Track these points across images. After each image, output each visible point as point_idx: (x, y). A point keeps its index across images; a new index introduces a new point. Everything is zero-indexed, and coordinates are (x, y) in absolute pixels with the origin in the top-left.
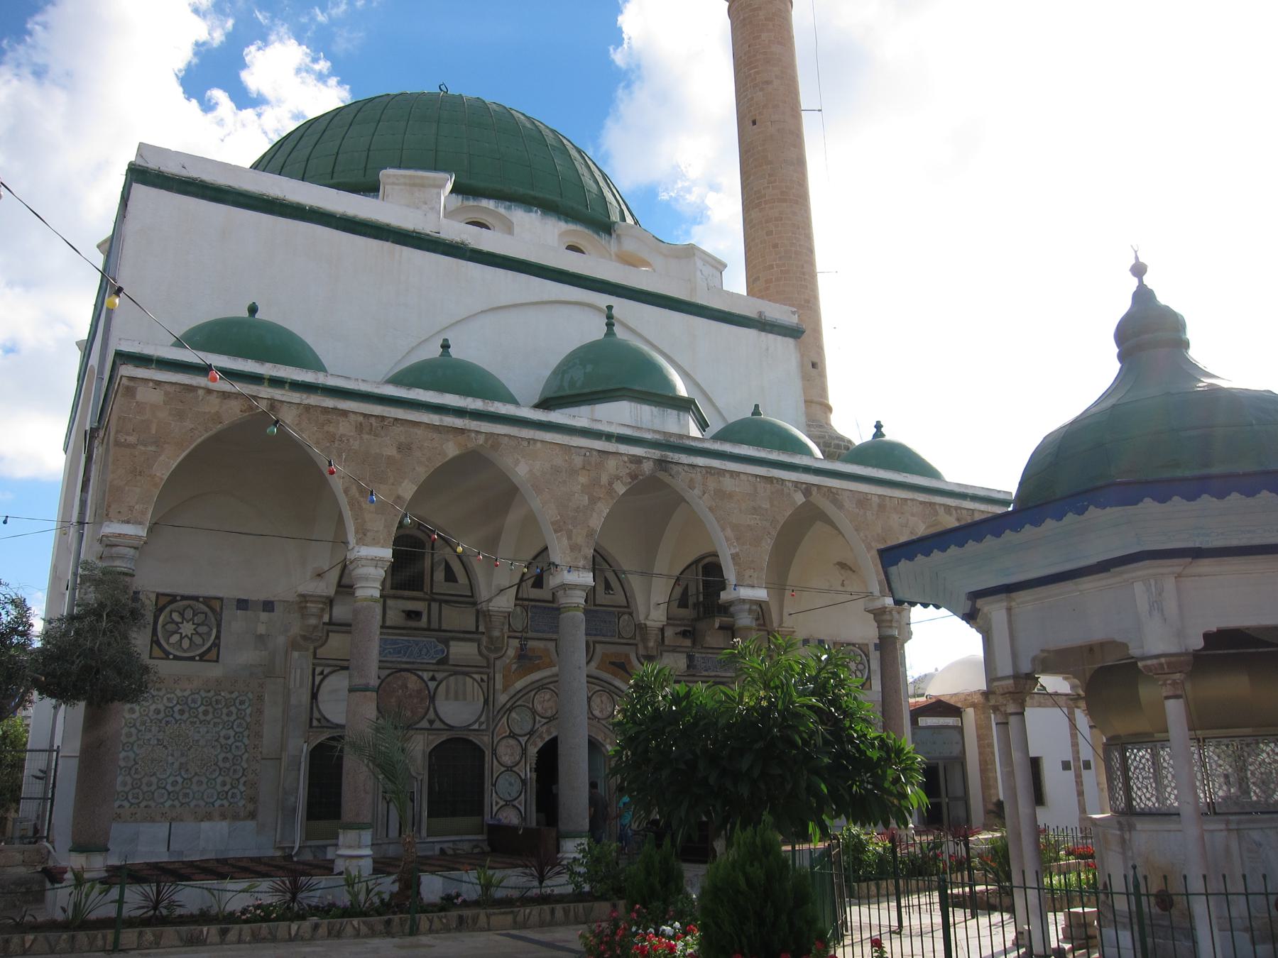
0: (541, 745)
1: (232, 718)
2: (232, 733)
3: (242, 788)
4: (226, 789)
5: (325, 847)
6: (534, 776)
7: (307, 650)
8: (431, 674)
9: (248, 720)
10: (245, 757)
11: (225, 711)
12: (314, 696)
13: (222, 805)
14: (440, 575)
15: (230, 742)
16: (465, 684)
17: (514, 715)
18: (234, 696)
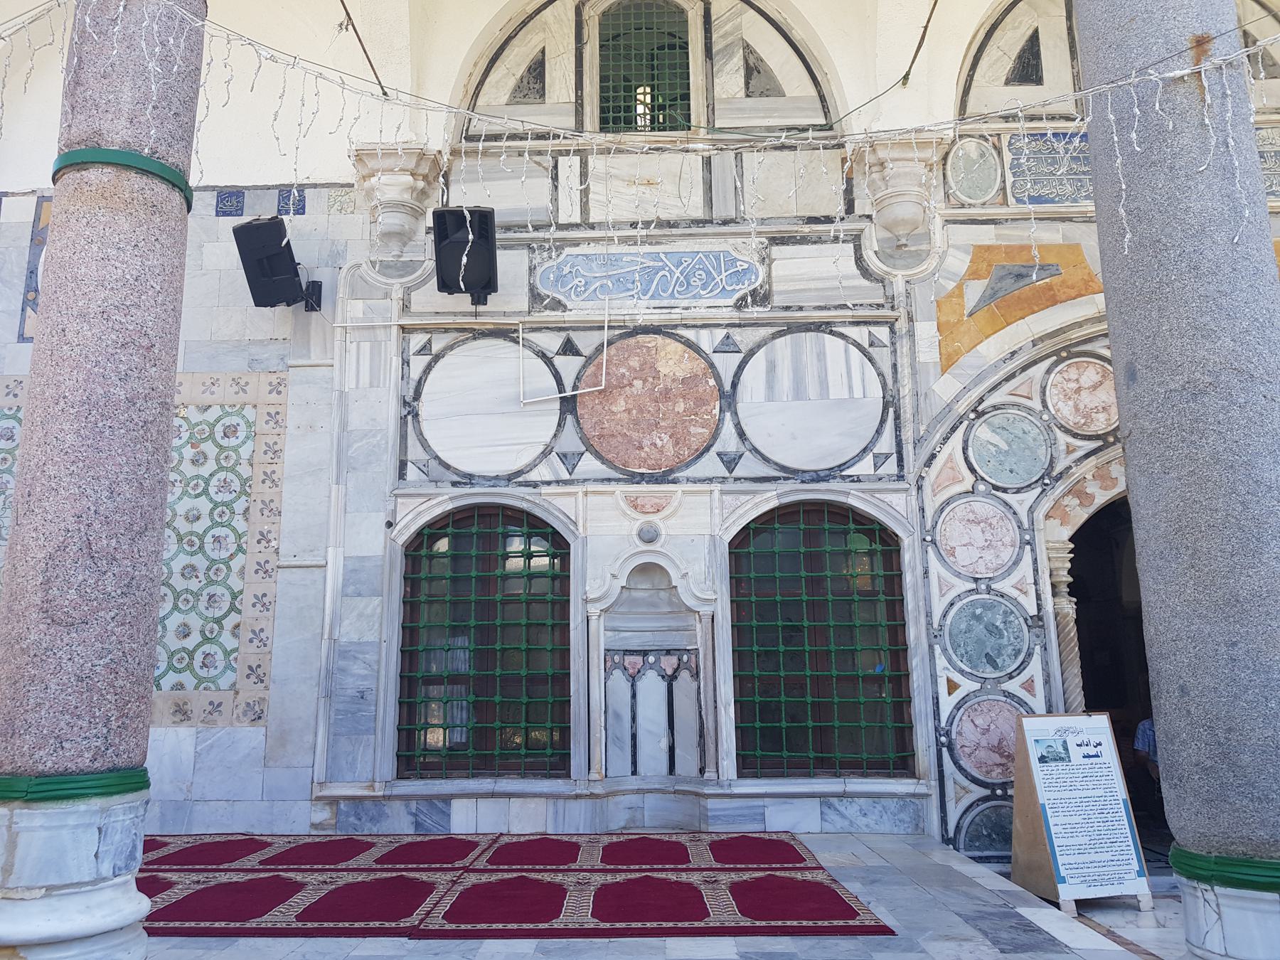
0: (1081, 515)
1: (205, 471)
2: (204, 505)
3: (228, 641)
4: (190, 643)
5: (447, 799)
6: (1069, 607)
7: (387, 295)
8: (720, 334)
9: (245, 470)
10: (236, 564)
11: (189, 452)
12: (410, 408)
13: (180, 686)
14: (730, 81)
15: (199, 527)
16: (821, 356)
17: (983, 432)
18: (211, 415)
